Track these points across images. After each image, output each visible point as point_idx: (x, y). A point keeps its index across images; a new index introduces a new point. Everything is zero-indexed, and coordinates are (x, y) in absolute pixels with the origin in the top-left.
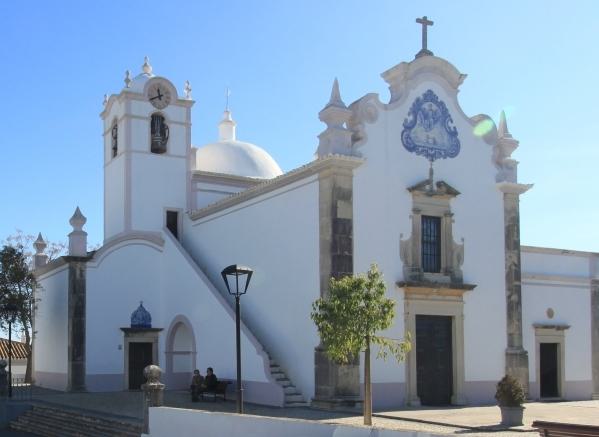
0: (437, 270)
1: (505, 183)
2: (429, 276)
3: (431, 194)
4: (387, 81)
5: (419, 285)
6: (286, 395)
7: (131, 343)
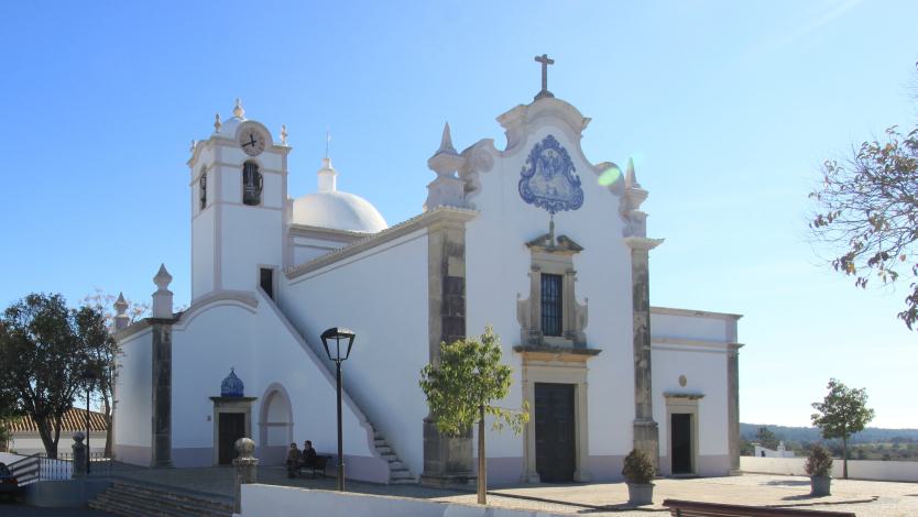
0: (558, 333)
1: (632, 238)
2: (549, 340)
3: (551, 250)
4: (503, 126)
5: (537, 350)
6: (393, 470)
7: (221, 414)
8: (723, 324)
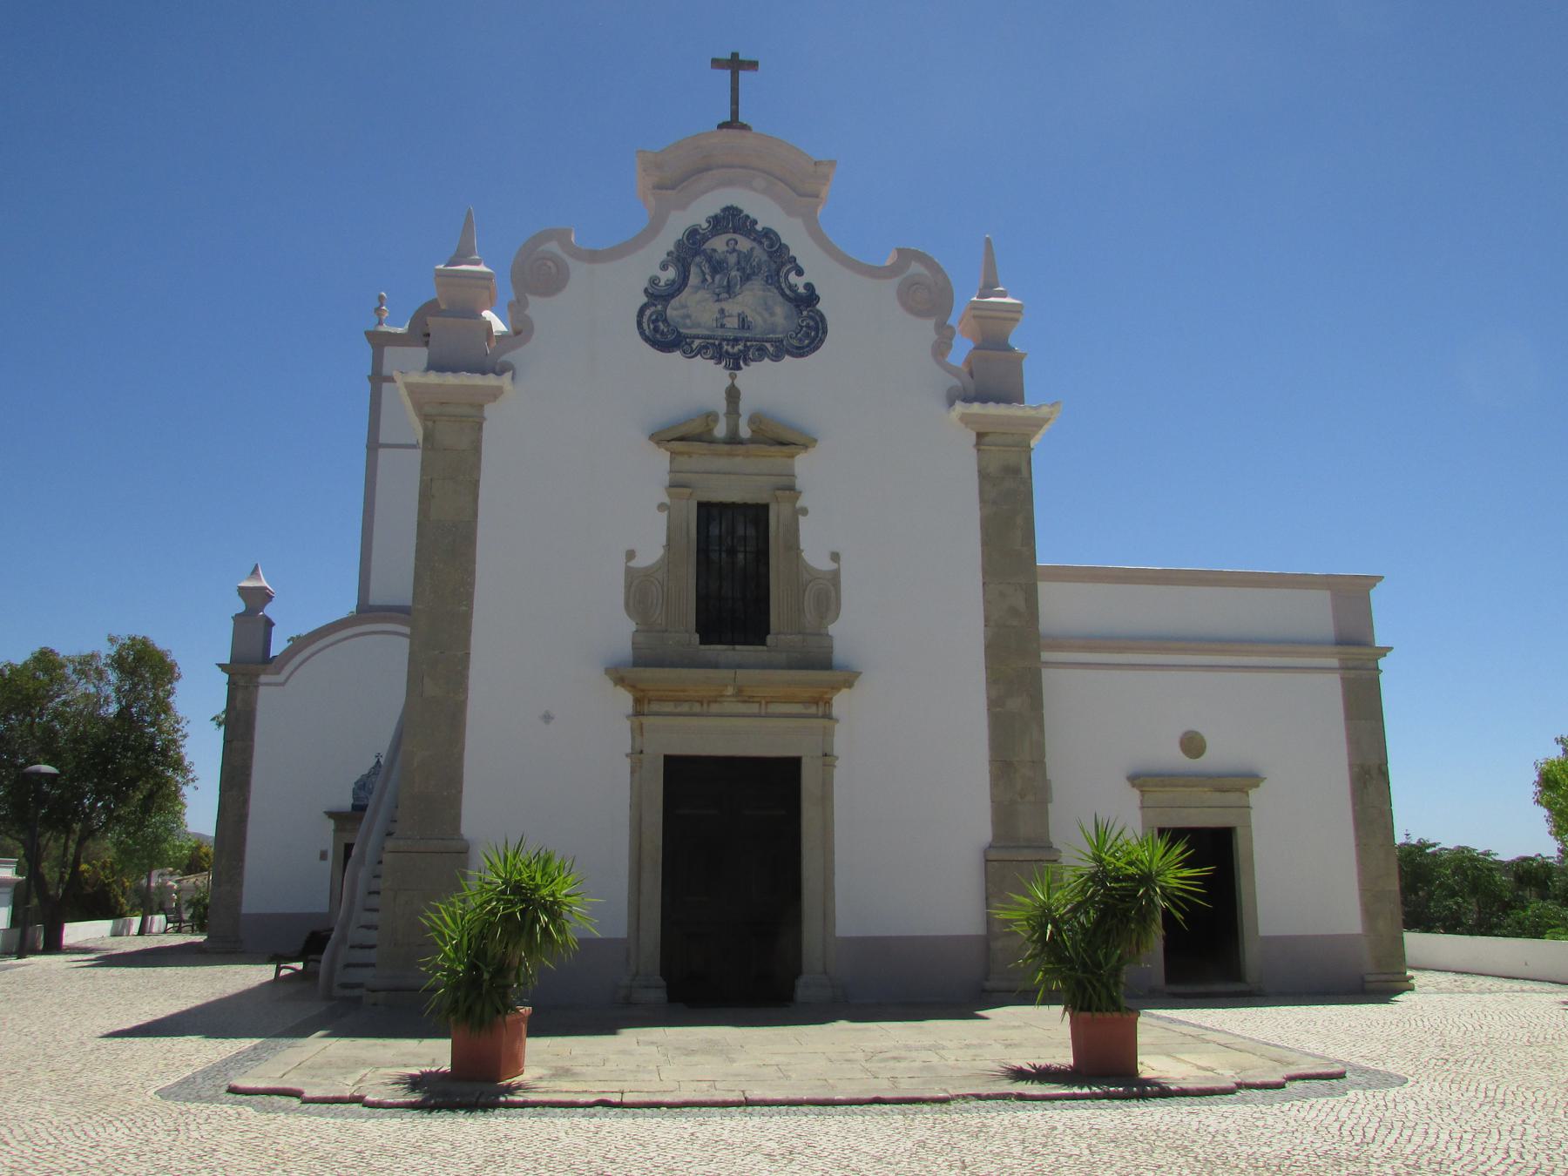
8: (1321, 600)
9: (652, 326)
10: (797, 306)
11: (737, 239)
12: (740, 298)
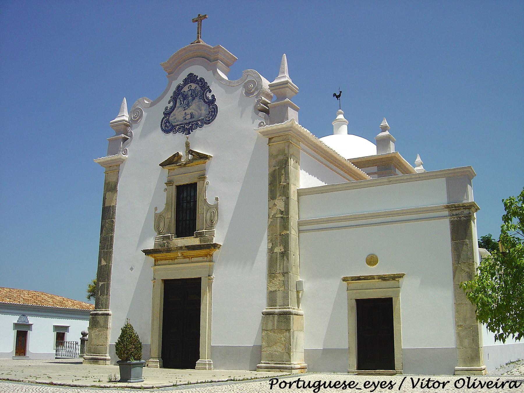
9: (165, 125)
10: (209, 105)
11: (191, 85)
12: (191, 107)
